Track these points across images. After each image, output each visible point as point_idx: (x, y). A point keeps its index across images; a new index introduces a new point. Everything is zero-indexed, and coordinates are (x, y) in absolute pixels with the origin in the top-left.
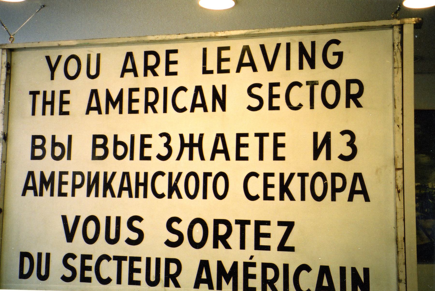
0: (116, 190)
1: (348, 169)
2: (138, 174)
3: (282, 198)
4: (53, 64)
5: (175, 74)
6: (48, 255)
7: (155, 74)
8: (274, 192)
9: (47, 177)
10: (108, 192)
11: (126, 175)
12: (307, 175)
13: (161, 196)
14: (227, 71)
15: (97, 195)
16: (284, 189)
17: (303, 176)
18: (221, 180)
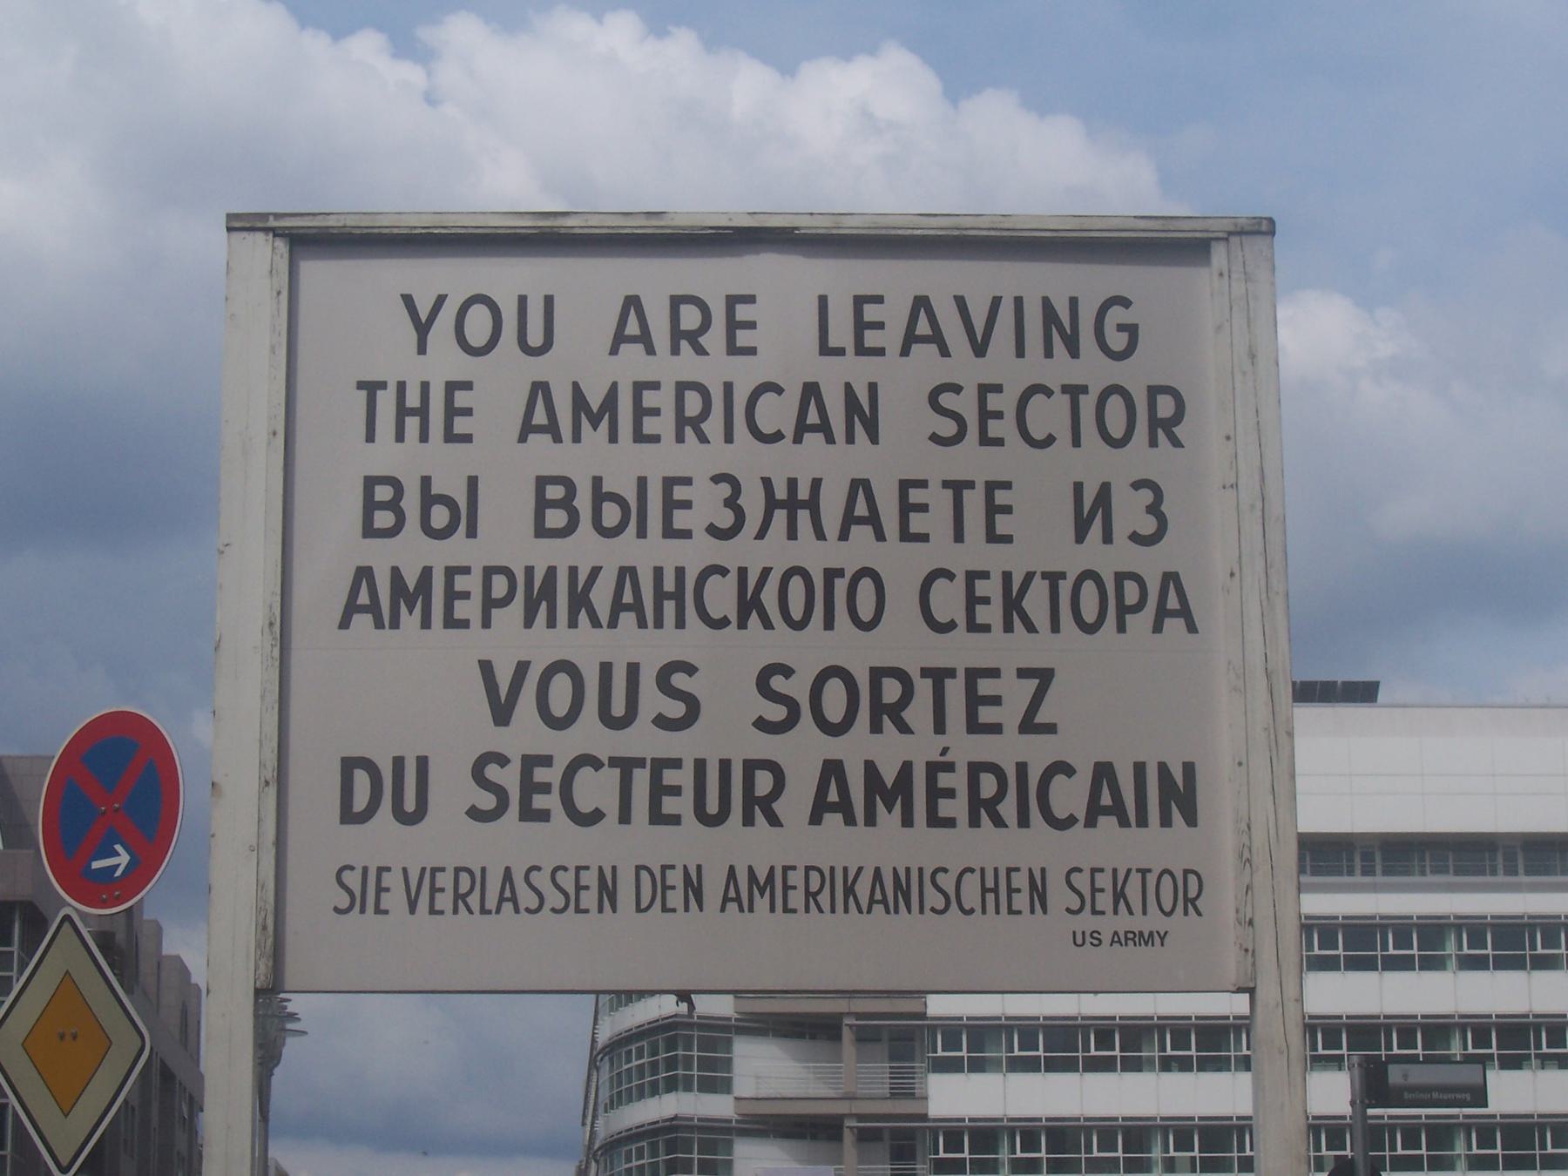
0: (603, 607)
1: (1150, 562)
2: (658, 572)
3: (1008, 627)
5: (752, 351)
6: (423, 763)
7: (700, 351)
8: (990, 614)
9: (411, 582)
10: (583, 617)
12: (1063, 575)
13: (723, 623)
14: (880, 352)
15: (552, 623)
16: (1013, 605)
17: (1053, 578)
18: (866, 585)
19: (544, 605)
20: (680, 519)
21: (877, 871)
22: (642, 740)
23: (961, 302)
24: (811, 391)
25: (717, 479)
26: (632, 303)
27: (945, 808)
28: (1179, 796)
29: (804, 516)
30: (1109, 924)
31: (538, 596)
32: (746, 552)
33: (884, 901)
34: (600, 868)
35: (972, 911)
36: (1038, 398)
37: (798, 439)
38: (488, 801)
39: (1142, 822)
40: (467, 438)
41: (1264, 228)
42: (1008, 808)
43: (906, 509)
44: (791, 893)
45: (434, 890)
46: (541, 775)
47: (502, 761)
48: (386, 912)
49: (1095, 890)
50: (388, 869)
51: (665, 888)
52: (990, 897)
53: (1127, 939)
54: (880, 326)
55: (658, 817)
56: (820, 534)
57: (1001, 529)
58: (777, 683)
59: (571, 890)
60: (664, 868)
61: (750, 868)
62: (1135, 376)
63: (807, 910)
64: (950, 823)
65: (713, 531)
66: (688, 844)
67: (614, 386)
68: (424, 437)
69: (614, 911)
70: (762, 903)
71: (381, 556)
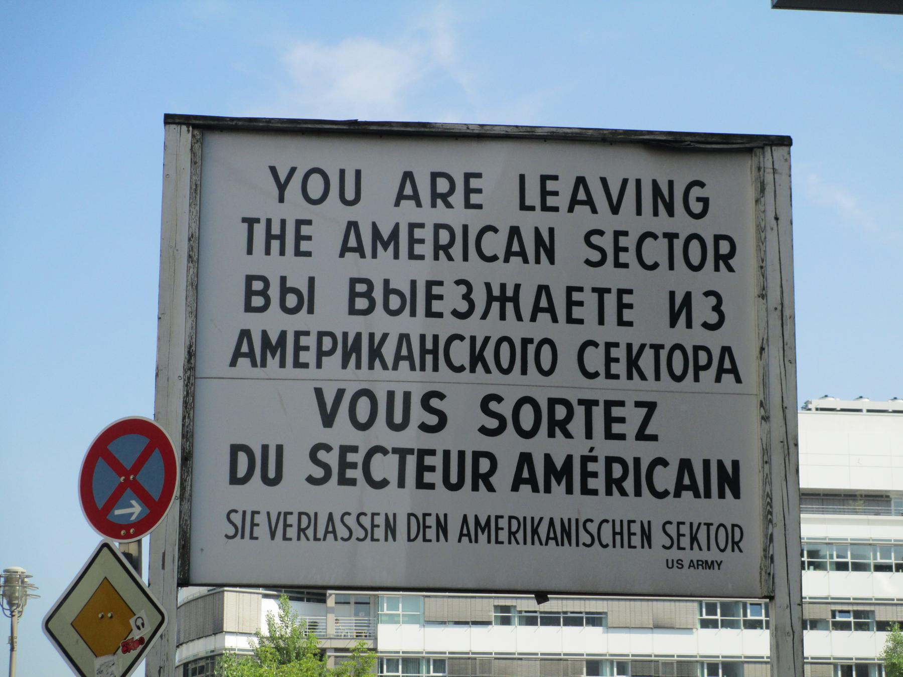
1: (715, 341)
2: (423, 338)
3: (630, 377)
4: (282, 179)
5: (479, 207)
6: (280, 449)
7: (449, 205)
8: (619, 368)
9: (274, 339)
10: (377, 363)
11: (404, 338)
13: (461, 369)
14: (555, 209)
15: (358, 366)
16: (633, 363)
17: (657, 348)
18: (546, 349)
19: (354, 355)
20: (436, 306)
21: (551, 520)
22: (411, 438)
23: (604, 181)
24: (515, 232)
25: (458, 282)
26: (408, 176)
27: (592, 483)
28: (730, 480)
29: (510, 306)
30: (687, 556)
31: (351, 350)
32: (473, 327)
33: (555, 538)
34: (386, 515)
35: (607, 546)
36: (649, 241)
37: (507, 260)
38: (319, 473)
39: (708, 495)
40: (308, 254)
41: (785, 142)
42: (629, 485)
43: (570, 304)
44: (500, 531)
45: (286, 526)
46: (351, 457)
47: (328, 448)
48: (257, 538)
49: (679, 535)
50: (258, 513)
51: (425, 527)
52: (618, 537)
53: (698, 565)
54: (556, 193)
55: (421, 484)
56: (519, 318)
57: (625, 318)
58: (493, 406)
59: (368, 526)
60: (425, 515)
61: (476, 517)
62: (707, 228)
63: (510, 543)
64: (595, 492)
65: (455, 313)
66: (440, 501)
67: (397, 226)
68: (282, 253)
69: (394, 540)
70: (483, 538)
71: (256, 324)
